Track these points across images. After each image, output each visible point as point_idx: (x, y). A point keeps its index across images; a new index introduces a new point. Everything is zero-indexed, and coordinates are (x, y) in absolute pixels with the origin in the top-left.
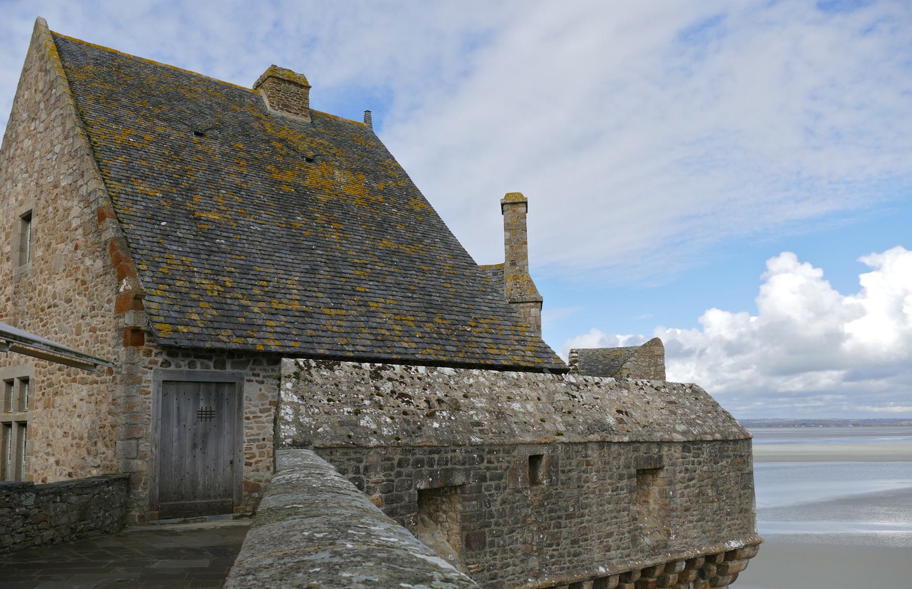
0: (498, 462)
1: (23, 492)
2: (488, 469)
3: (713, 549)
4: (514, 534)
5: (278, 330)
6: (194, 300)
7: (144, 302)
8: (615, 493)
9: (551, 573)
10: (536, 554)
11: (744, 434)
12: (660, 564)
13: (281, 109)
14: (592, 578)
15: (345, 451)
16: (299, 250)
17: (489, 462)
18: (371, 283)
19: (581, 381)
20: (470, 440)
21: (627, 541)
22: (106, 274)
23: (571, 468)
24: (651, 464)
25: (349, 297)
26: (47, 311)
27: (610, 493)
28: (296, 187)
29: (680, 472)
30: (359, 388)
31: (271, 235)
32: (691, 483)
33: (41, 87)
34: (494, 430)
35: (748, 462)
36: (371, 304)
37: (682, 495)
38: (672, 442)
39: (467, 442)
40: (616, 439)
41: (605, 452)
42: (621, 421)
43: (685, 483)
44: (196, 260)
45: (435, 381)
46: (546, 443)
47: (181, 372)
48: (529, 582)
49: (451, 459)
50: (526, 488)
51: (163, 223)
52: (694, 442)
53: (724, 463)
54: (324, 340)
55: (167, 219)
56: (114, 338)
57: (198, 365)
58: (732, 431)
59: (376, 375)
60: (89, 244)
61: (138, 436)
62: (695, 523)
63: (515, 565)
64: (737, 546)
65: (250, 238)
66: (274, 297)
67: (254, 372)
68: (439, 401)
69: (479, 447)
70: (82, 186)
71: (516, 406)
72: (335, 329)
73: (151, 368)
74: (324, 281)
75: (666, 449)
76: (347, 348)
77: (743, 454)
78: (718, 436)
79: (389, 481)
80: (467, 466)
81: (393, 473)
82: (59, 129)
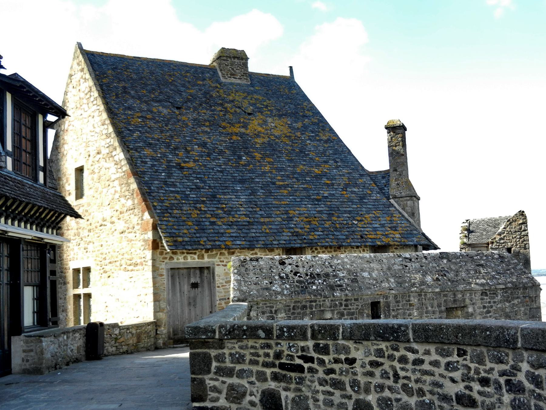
0: (351, 305)
2: (345, 309)
5: (234, 235)
6: (184, 221)
13: (230, 77)
15: (264, 302)
18: (291, 198)
19: (414, 256)
24: (457, 304)
25: (275, 209)
28: (242, 135)
29: (480, 308)
30: (273, 270)
31: (227, 172)
32: (488, 315)
34: (349, 289)
35: (535, 301)
36: (290, 212)
45: (317, 263)
47: (180, 263)
51: (163, 174)
53: (516, 302)
67: (221, 260)
68: (318, 275)
71: (366, 274)
72: (268, 231)
73: (163, 262)
76: (274, 242)
81: (290, 313)
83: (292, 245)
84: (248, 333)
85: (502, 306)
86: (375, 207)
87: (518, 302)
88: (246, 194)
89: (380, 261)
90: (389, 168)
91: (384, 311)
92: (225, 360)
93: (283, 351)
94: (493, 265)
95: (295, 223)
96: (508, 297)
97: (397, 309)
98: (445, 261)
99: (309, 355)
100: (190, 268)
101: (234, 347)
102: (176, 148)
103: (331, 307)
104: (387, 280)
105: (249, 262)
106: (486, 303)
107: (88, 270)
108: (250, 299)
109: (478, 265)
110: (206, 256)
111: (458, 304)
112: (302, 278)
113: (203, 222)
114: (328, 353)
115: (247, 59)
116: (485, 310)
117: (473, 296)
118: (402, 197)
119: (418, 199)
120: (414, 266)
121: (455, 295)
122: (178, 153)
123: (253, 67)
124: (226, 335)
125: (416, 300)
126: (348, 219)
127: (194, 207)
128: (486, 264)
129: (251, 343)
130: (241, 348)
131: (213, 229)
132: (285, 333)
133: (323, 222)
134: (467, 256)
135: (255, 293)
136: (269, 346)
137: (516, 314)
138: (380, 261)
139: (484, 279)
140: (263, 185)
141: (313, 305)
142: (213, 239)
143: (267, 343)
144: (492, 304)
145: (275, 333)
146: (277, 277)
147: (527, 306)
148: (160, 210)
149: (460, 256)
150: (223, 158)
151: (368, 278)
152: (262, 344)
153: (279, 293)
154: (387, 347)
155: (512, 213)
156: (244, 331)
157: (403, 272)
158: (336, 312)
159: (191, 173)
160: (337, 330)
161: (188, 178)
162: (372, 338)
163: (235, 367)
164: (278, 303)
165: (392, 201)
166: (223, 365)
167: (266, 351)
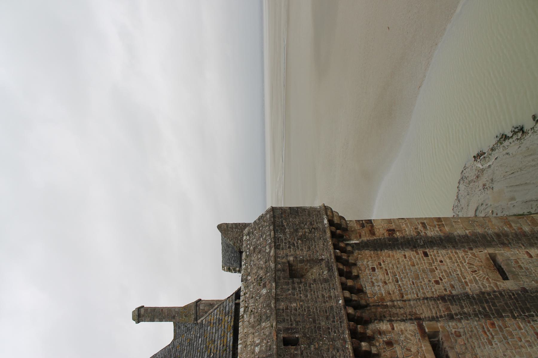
3: (328, 234)
4: (324, 355)
8: (302, 292)
9: (343, 333)
10: (334, 341)
11: (270, 212)
14: (345, 308)
19: (243, 304)
21: (326, 285)
23: (289, 319)
24: (286, 269)
27: (302, 295)
29: (290, 251)
32: (296, 245)
35: (285, 210)
37: (302, 250)
38: (275, 255)
40: (274, 291)
41: (281, 298)
42: (264, 286)
43: (296, 249)
46: (277, 336)
48: (348, 347)
50: (301, 348)
52: (275, 243)
53: (285, 224)
58: (269, 218)
62: (316, 244)
63: (340, 355)
64: (326, 220)
71: (257, 350)
75: (279, 259)
78: (272, 227)
85: (289, 234)
86: (201, 336)
87: (285, 222)
89: (246, 335)
90: (172, 323)
91: (292, 333)
94: (255, 240)
96: (281, 229)
98: (249, 278)
104: (263, 329)
109: (254, 251)
111: (286, 268)
116: (292, 247)
117: (280, 255)
118: (197, 313)
119: (200, 300)
121: (279, 270)
125: (283, 304)
128: (254, 245)
137: (295, 224)
138: (246, 335)
147: (289, 216)
149: (246, 266)
151: (261, 347)
157: (257, 314)
165: (199, 321)
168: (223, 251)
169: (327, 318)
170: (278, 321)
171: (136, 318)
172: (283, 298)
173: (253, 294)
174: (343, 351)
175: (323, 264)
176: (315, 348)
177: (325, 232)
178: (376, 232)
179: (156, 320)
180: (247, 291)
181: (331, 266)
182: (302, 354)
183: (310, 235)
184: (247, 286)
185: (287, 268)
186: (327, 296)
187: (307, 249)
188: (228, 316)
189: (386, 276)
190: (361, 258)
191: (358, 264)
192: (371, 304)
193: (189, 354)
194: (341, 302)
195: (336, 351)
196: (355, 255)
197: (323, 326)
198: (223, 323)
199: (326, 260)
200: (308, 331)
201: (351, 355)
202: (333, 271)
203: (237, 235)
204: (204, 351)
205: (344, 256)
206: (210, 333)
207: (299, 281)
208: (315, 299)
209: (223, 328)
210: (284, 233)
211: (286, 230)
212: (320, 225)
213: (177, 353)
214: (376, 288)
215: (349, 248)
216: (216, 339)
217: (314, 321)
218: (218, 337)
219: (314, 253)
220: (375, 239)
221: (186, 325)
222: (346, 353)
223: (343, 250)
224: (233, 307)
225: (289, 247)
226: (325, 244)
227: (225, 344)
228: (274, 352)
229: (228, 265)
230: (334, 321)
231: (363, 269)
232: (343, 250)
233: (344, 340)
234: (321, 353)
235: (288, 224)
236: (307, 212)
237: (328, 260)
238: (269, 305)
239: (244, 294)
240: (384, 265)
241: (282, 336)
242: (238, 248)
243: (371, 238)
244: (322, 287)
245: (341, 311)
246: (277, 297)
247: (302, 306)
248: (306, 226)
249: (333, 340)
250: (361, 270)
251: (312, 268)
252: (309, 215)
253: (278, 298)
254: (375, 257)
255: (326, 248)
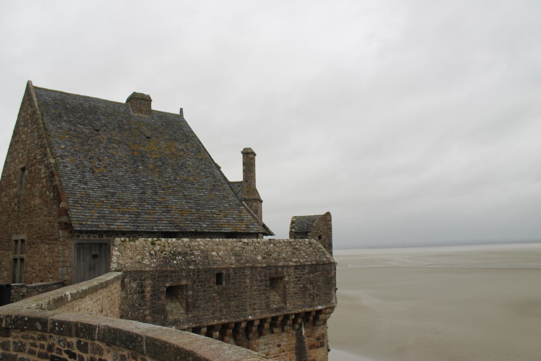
0: (202, 275)
1: (22, 287)
3: (308, 309)
7: (69, 212)
8: (258, 287)
9: (226, 318)
11: (329, 261)
12: (280, 316)
13: (138, 112)
14: (245, 321)
16: (138, 183)
17: (198, 275)
19: (250, 241)
20: (189, 267)
21: (264, 305)
22: (55, 199)
23: (236, 278)
25: (159, 204)
26: (32, 212)
27: (256, 287)
29: (293, 278)
30: (145, 249)
32: (299, 282)
33: (29, 113)
34: (201, 264)
37: (294, 287)
39: (187, 268)
40: (259, 265)
42: (264, 258)
44: (91, 191)
45: (179, 245)
46: (224, 268)
49: (180, 274)
51: (79, 176)
52: (300, 266)
53: (317, 273)
54: (144, 225)
55: (80, 173)
56: (57, 226)
57: (92, 236)
58: (323, 260)
59: (153, 243)
60: (48, 186)
61: (67, 266)
62: (300, 299)
65: (117, 179)
66: (125, 206)
69: (193, 270)
70: (45, 160)
71: (214, 253)
74: (149, 197)
75: (286, 269)
77: (328, 270)
78: (314, 262)
79: (154, 283)
80: (187, 278)
81: (155, 281)
82: (36, 134)
83: (168, 230)
84: (28, 324)
87: (319, 273)
88: (140, 193)
89: (226, 245)
90: (242, 180)
92: (9, 347)
93: (54, 344)
94: (304, 249)
95: (172, 214)
97: (236, 279)
98: (272, 245)
99: (73, 351)
100: (92, 244)
101: (18, 336)
102: (91, 158)
103: (186, 276)
104: (229, 258)
105: (127, 243)
106: (298, 274)
107: (23, 241)
108: (125, 270)
110: (92, 236)
112: (166, 255)
113: (103, 211)
114: (86, 352)
115: (151, 101)
116: (297, 279)
118: (250, 200)
119: (261, 201)
120: (249, 249)
121: (276, 269)
122: (93, 161)
123: (155, 106)
124: (11, 324)
126: (210, 213)
127: (99, 200)
128: (300, 248)
129: (31, 334)
130: (23, 337)
131: (111, 216)
132: (57, 327)
133: (192, 215)
134: (288, 242)
135: (129, 266)
136: (44, 338)
138: (226, 245)
139: (297, 258)
140: (152, 186)
141: (173, 275)
142: (109, 223)
143: (43, 335)
144: (302, 275)
145: (49, 326)
146: (147, 254)
148: (73, 201)
150: (125, 167)
152: (39, 335)
153: (148, 266)
154: (128, 354)
155: (322, 212)
156: (26, 321)
157: (242, 252)
158: (190, 280)
159: (100, 176)
160: (94, 331)
161: (97, 179)
162: (118, 343)
163: (17, 355)
164: (147, 273)
165: (244, 202)
166: (7, 352)
167: (42, 342)
168: (309, 216)
169: (237, 307)
170: (235, 269)
171: (246, 151)
172: (253, 273)
173: (258, 249)
174: (212, 318)
175: (282, 305)
176: (214, 297)
177: (311, 306)
178: (312, 350)
179: (244, 167)
180: (261, 244)
181: (280, 311)
182: (211, 287)
183: (308, 294)
184: (264, 244)
185: (278, 275)
186: (256, 307)
187: (295, 292)
188: (245, 227)
189: (273, 356)
190: (289, 336)
191: (284, 333)
192: (249, 342)
193: (216, 197)
194: (250, 317)
195: (213, 312)
196: (292, 331)
197: (231, 303)
198: (240, 223)
199: (286, 307)
200: (227, 292)
201: (209, 324)
202: (276, 312)
203: (321, 230)
204: (219, 209)
205: (289, 322)
206: (232, 213)
207: (267, 285)
208: (252, 297)
209: (236, 223)
210: (309, 273)
211: (312, 274)
212: (316, 302)
213: (217, 187)
214: (263, 347)
215: (297, 326)
216: (228, 218)
217: (235, 297)
218: (229, 220)
219: (291, 298)
220: (305, 349)
221: (241, 192)
222: (211, 320)
223: (295, 321)
224: (252, 231)
225: (296, 277)
226: (300, 307)
227: (223, 226)
228: (212, 266)
229: (297, 222)
230: (235, 311)
231: (280, 337)
232: (295, 321)
233: (220, 319)
234: (211, 301)
235: (317, 276)
236: (328, 292)
237: (286, 309)
238: (248, 262)
239: (258, 242)
240: (283, 355)
241: (224, 272)
242: (310, 231)
243: (306, 346)
244: (262, 303)
245: (243, 317)
246: (254, 268)
247: (247, 287)
248: (315, 291)
249: (221, 310)
250: (279, 335)
251: (280, 295)
252: (326, 294)
253: (253, 269)
254: (290, 347)
255: (296, 307)
